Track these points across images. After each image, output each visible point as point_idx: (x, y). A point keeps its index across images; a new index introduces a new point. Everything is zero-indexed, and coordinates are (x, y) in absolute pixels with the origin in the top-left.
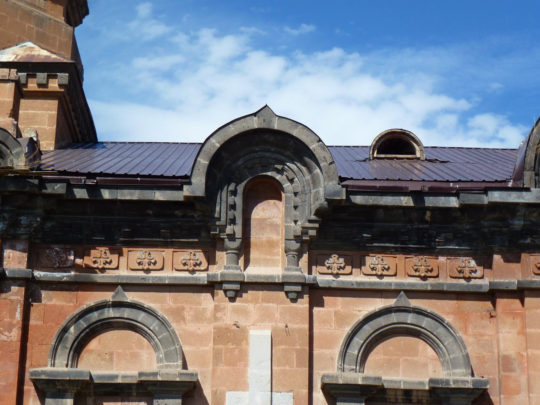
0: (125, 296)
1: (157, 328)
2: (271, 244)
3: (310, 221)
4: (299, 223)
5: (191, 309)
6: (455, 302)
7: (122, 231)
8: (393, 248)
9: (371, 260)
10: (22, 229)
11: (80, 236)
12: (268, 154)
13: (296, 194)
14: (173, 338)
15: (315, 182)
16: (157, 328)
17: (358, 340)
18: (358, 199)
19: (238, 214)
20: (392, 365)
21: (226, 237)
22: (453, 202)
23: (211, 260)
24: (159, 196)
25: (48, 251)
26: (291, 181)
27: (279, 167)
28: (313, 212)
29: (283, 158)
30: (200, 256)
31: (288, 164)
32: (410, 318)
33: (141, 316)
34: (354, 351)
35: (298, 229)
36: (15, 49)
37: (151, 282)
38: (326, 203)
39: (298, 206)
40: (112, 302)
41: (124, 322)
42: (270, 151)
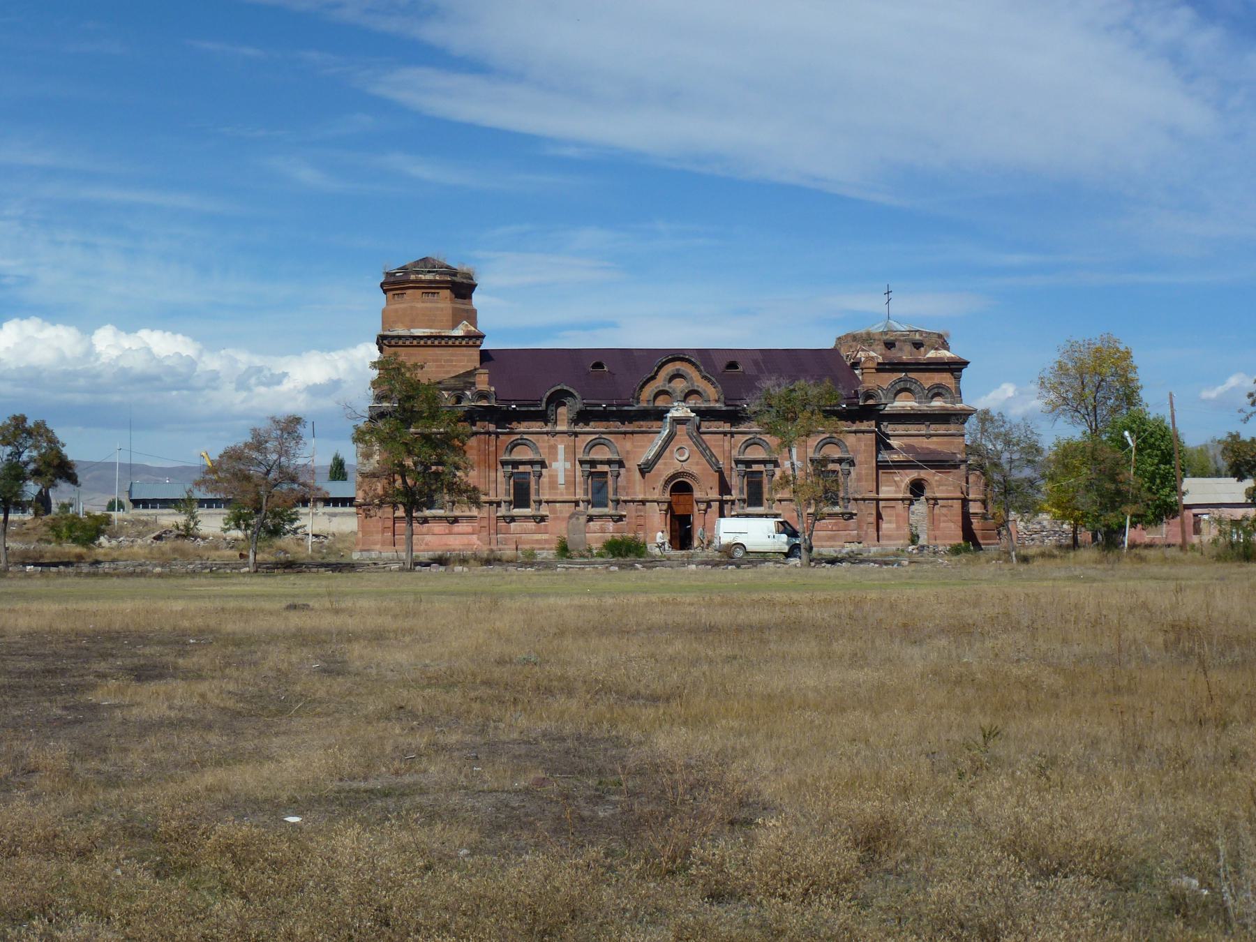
2: (563, 420)
9: (592, 424)
14: (537, 448)
17: (588, 447)
18: (588, 408)
19: (554, 412)
20: (596, 453)
22: (615, 409)
23: (546, 425)
24: (532, 409)
30: (543, 424)
32: (602, 440)
33: (528, 442)
34: (587, 450)
35: (571, 416)
36: (461, 326)
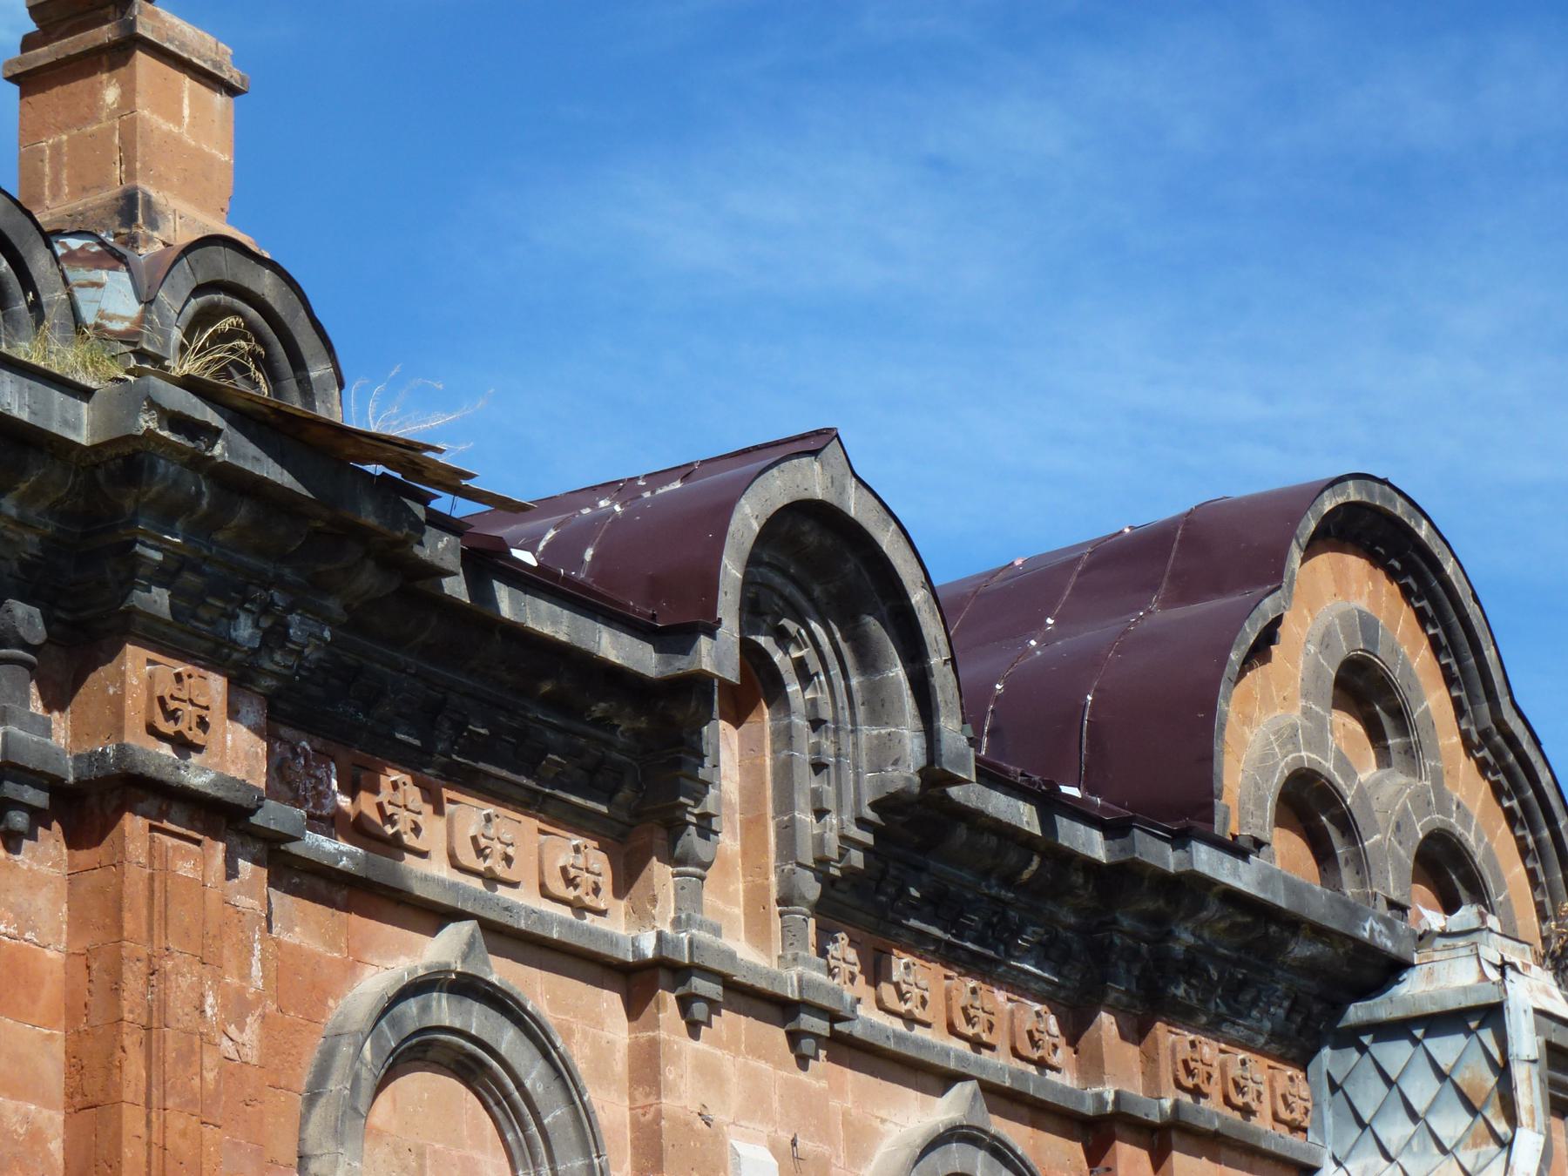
0: (486, 962)
1: (540, 1089)
3: (861, 823)
4: (832, 819)
5: (585, 1034)
6: (1029, 1129)
7: (470, 732)
8: (937, 940)
10: (278, 657)
11: (361, 716)
12: (777, 580)
13: (816, 724)
15: (879, 709)
16: (540, 1089)
21: (694, 820)
25: (278, 745)
26: (805, 676)
27: (791, 626)
28: (867, 800)
29: (803, 602)
31: (814, 625)
33: (508, 1040)
37: (522, 925)
38: (917, 779)
39: (826, 766)
40: (458, 974)
41: (462, 1048)
42: (784, 572)
